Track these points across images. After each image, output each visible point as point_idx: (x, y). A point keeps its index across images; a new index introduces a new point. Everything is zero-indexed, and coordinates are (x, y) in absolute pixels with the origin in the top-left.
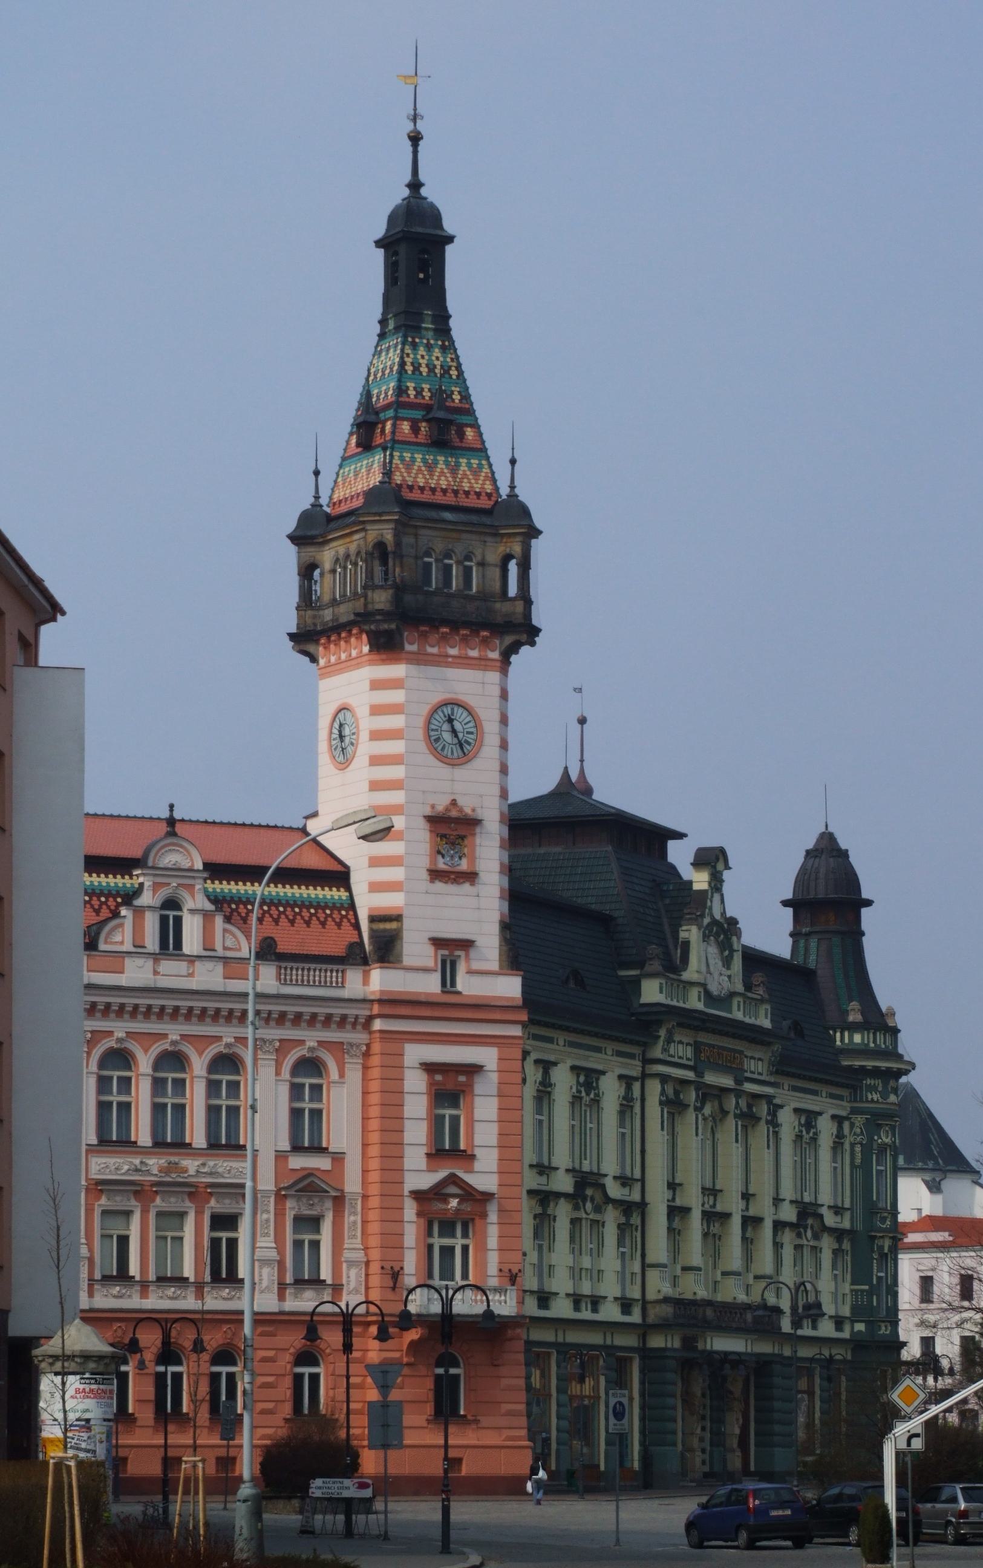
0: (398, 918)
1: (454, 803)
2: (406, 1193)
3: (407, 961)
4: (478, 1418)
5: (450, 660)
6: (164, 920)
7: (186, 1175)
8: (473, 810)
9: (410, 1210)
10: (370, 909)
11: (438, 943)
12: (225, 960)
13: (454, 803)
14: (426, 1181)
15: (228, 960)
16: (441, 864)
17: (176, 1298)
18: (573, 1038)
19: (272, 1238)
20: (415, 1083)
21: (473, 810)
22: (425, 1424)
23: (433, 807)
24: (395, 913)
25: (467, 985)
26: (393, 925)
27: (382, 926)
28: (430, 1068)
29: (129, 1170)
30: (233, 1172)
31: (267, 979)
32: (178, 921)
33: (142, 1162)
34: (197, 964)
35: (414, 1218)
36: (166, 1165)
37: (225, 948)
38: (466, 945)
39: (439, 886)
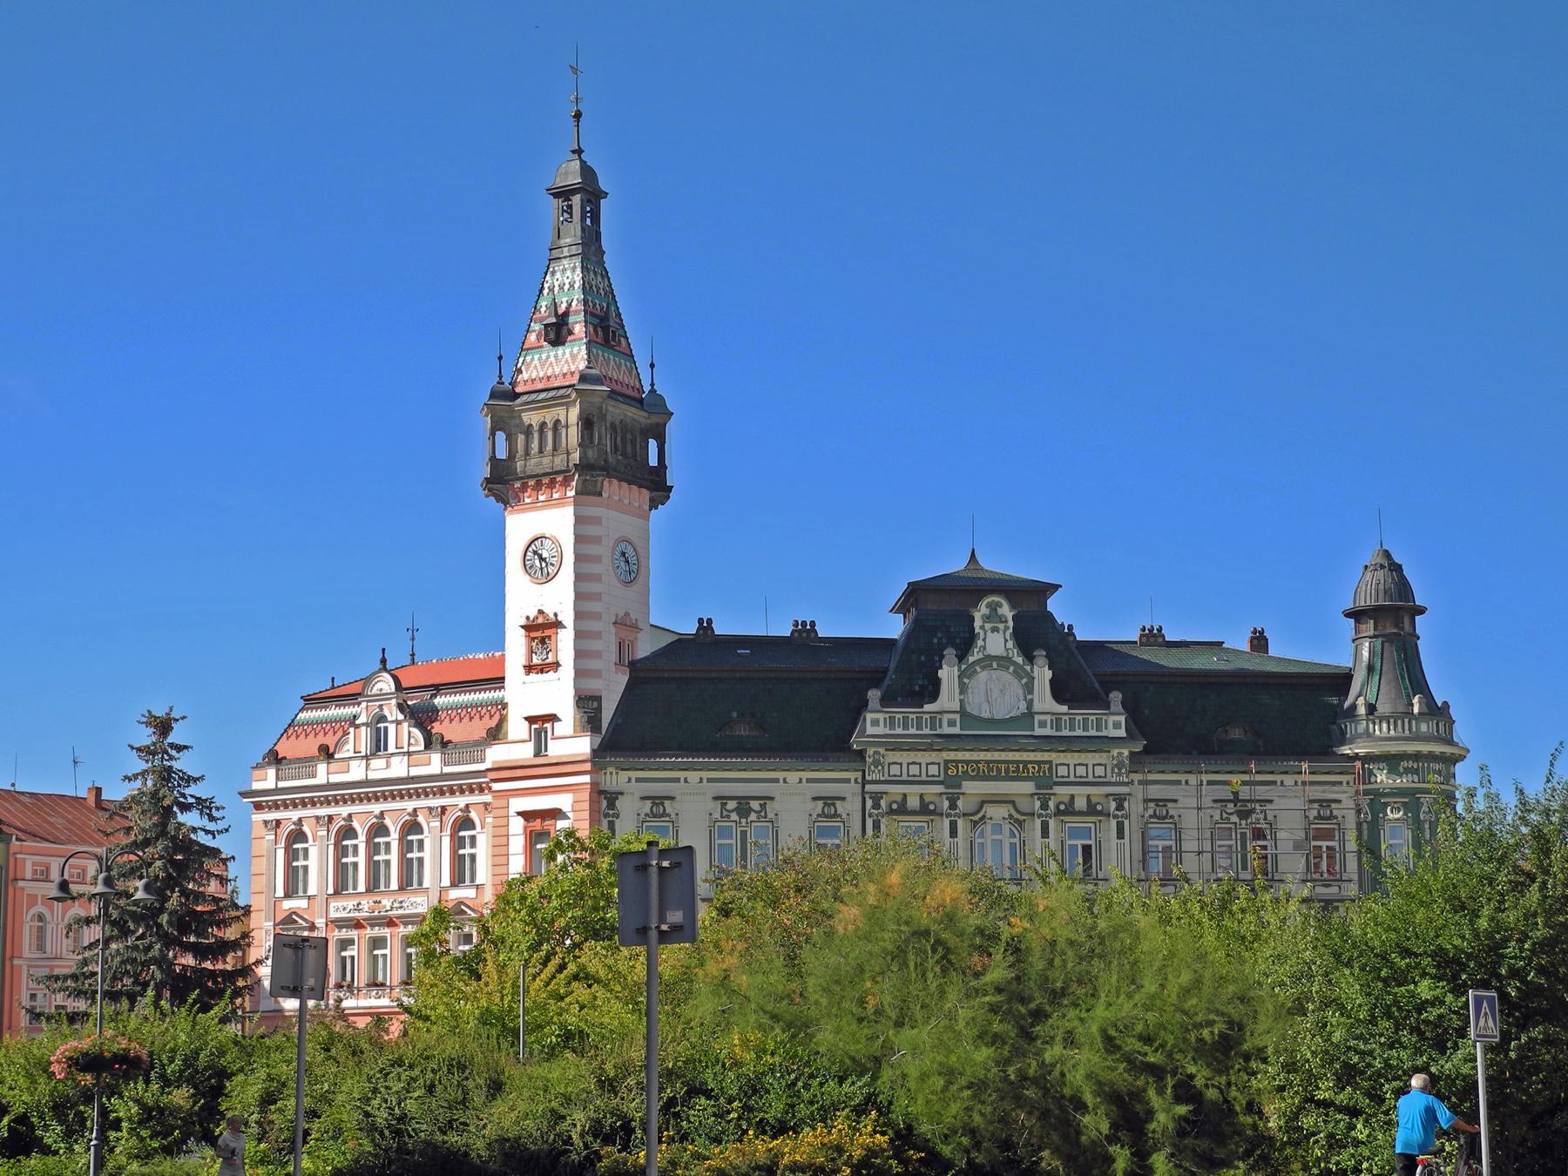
1: (541, 612)
3: (511, 737)
8: (556, 615)
11: (531, 720)
12: (409, 754)
13: (541, 612)
16: (536, 660)
18: (706, 775)
20: (517, 825)
23: (528, 618)
25: (556, 750)
28: (527, 815)
31: (435, 764)
34: (394, 760)
38: (553, 718)
39: (533, 676)
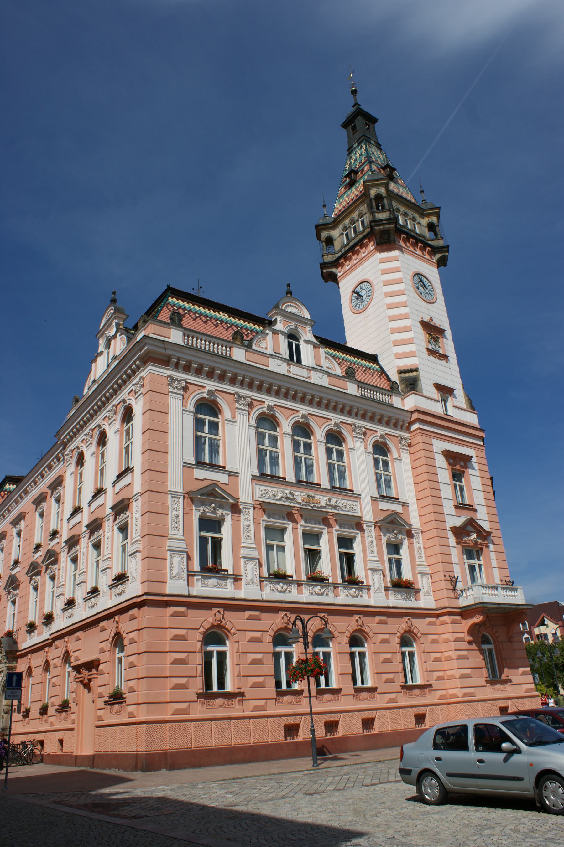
0: (416, 370)
2: (448, 529)
4: (510, 677)
5: (416, 255)
6: (290, 345)
7: (319, 506)
9: (452, 540)
10: (398, 367)
13: (431, 319)
14: (458, 522)
15: (330, 375)
17: (322, 594)
19: (376, 554)
21: (440, 326)
22: (485, 684)
24: (414, 368)
26: (414, 374)
27: (407, 375)
29: (282, 497)
30: (348, 507)
31: (352, 389)
32: (298, 348)
33: (291, 493)
35: (455, 545)
36: (306, 496)
37: (328, 368)
